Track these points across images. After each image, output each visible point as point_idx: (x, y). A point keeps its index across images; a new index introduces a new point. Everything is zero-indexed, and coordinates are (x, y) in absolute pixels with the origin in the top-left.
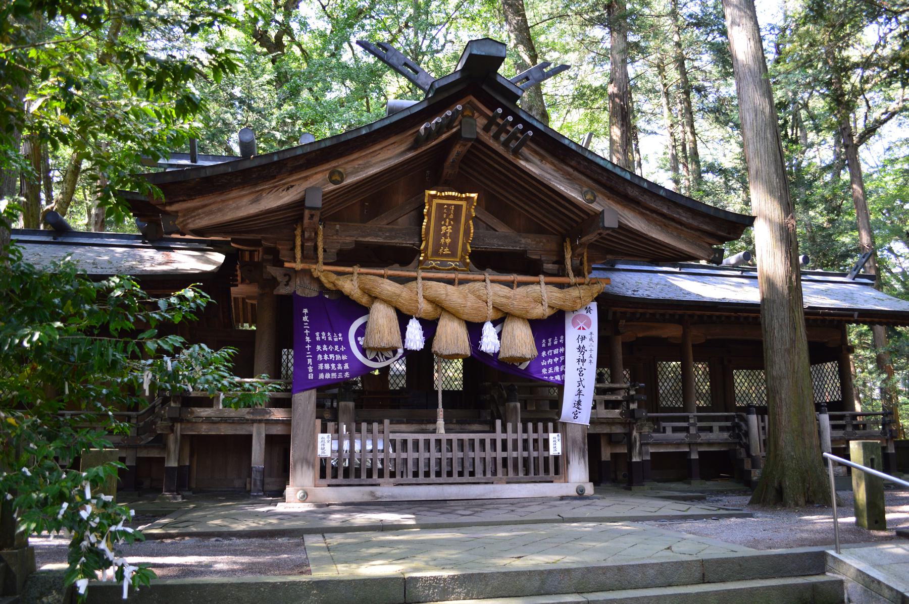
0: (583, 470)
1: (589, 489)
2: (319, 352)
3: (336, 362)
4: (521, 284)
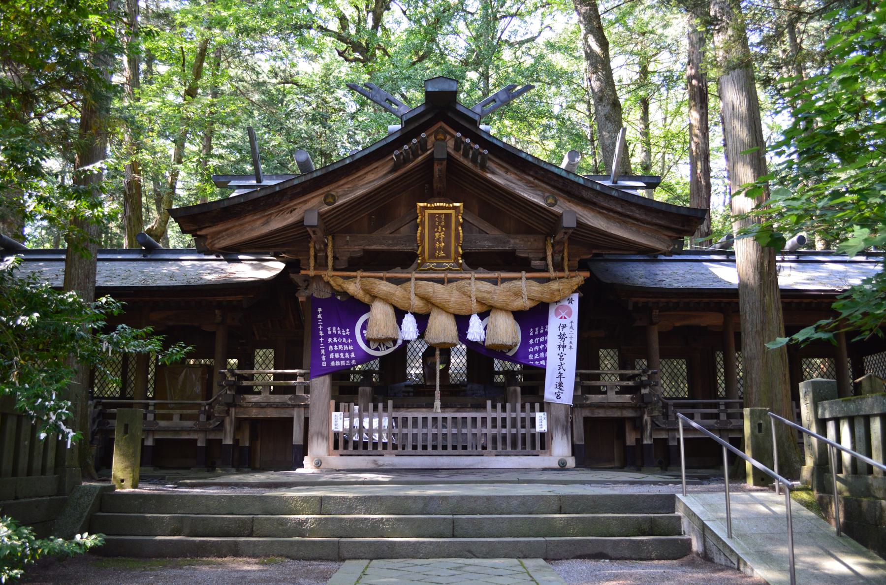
0: (566, 445)
1: (571, 462)
2: (331, 344)
3: (344, 352)
4: (504, 280)
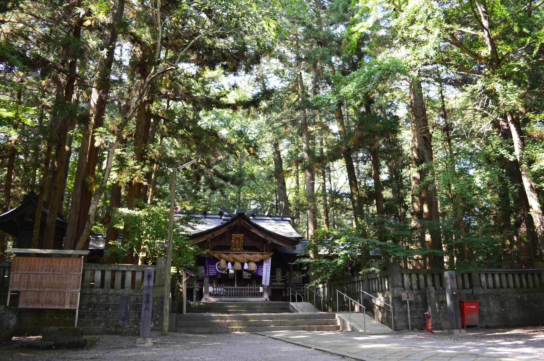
1: (268, 299)
